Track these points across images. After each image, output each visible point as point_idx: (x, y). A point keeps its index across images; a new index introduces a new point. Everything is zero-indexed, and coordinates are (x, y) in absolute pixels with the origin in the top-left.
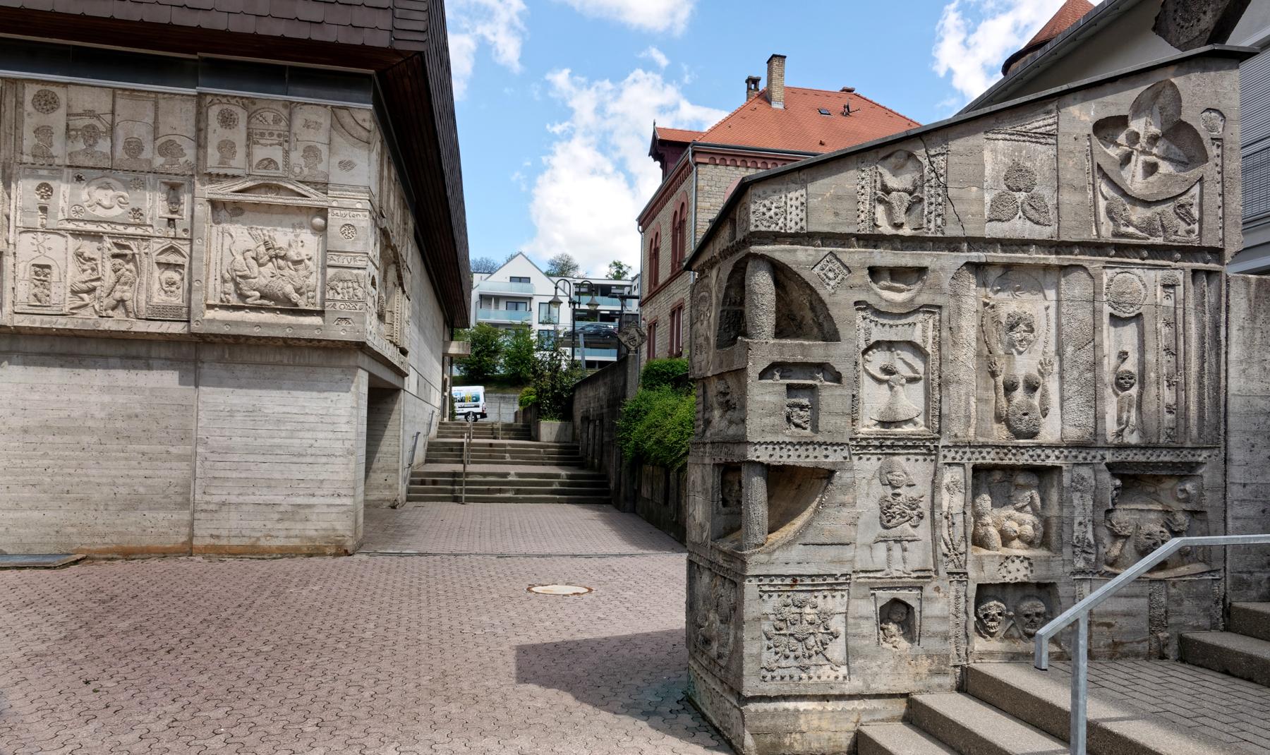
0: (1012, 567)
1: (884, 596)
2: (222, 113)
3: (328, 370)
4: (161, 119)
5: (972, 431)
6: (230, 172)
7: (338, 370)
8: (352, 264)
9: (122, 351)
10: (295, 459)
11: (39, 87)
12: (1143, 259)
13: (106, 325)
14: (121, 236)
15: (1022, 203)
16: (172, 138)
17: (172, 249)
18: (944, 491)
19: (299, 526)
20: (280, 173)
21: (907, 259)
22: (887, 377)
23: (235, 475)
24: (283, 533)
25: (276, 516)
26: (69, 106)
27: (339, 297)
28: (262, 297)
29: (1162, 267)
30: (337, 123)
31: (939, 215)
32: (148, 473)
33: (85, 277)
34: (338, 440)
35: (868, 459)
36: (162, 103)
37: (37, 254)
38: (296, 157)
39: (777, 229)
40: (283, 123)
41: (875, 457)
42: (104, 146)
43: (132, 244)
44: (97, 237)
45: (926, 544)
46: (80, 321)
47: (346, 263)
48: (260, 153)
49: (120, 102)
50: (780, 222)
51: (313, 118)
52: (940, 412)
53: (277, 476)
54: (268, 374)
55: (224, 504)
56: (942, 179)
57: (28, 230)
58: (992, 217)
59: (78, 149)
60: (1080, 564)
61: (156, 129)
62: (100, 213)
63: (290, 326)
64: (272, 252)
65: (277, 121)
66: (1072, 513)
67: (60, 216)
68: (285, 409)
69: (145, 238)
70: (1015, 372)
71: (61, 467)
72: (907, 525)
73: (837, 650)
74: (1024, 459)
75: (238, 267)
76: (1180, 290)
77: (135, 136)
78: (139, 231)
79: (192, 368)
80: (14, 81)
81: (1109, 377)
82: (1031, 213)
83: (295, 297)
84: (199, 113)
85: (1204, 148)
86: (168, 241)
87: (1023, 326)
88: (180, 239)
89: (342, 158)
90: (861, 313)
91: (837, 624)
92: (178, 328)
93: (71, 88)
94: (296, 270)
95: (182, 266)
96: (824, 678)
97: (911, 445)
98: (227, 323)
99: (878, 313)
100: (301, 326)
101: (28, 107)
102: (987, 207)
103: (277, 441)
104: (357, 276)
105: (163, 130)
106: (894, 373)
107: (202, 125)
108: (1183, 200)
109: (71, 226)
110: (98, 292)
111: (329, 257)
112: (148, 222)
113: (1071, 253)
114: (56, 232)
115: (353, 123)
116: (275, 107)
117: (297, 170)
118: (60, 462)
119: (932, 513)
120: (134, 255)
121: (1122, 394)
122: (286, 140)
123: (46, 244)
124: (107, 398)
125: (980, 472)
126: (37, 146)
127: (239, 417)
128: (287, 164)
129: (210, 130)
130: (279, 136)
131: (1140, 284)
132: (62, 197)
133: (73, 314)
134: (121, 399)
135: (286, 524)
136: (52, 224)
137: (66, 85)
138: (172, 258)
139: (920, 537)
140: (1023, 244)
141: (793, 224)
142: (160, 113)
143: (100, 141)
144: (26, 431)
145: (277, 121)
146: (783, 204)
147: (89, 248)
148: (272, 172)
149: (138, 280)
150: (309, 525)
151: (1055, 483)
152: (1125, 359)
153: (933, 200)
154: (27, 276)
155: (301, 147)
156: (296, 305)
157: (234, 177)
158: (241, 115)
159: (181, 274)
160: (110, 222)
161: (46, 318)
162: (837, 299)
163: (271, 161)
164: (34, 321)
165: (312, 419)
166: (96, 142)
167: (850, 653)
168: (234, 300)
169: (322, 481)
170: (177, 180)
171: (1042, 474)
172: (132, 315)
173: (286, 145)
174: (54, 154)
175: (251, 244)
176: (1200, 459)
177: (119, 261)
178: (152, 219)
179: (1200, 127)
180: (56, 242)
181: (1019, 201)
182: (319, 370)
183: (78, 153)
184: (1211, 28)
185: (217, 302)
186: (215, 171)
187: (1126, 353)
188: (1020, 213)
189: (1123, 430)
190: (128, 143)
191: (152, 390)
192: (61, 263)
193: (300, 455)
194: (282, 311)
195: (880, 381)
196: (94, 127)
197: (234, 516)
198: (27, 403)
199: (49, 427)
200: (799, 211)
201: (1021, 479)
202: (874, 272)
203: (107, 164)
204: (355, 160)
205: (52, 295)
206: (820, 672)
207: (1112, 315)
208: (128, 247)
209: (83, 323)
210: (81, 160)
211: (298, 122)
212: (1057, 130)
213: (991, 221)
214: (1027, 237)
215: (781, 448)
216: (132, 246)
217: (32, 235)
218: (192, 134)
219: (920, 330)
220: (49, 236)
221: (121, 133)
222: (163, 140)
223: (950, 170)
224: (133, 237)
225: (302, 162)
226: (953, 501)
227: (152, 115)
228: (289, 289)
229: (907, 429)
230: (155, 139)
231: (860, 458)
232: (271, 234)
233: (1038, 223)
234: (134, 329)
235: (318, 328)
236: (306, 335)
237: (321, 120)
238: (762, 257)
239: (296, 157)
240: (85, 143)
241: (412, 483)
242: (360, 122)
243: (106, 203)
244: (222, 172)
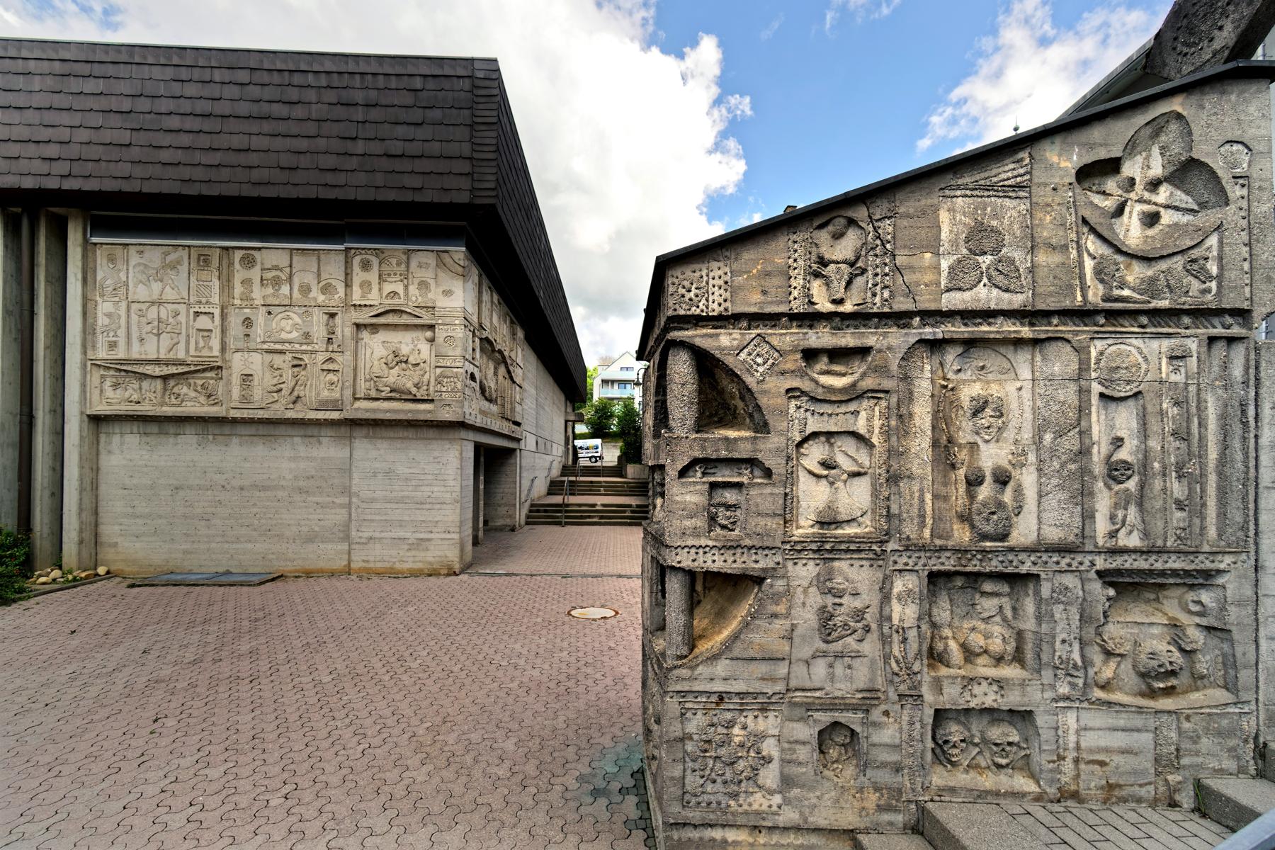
0: (977, 690)
1: (823, 719)
2: (362, 261)
3: (439, 442)
5: (927, 533)
6: (368, 303)
7: (447, 442)
8: (453, 365)
9: (302, 432)
10: (418, 506)
11: (244, 252)
12: (1143, 327)
13: (291, 415)
14: (297, 351)
15: (988, 268)
17: (330, 360)
18: (894, 601)
19: (423, 554)
20: (402, 301)
21: (848, 339)
22: (825, 472)
23: (377, 518)
24: (411, 559)
25: (406, 547)
26: (262, 264)
27: (444, 389)
28: (391, 391)
29: (1168, 335)
30: (441, 264)
31: (886, 287)
32: (321, 517)
33: (275, 381)
35: (805, 565)
36: (323, 257)
38: (413, 289)
39: (698, 312)
40: (403, 266)
41: (811, 563)
42: (285, 289)
43: (305, 357)
44: (282, 352)
45: (873, 662)
47: (449, 364)
48: (388, 288)
49: (295, 258)
50: (701, 304)
51: (424, 260)
52: (888, 512)
53: (406, 518)
54: (399, 446)
55: (371, 538)
56: (888, 246)
57: (238, 351)
58: (949, 285)
60: (1064, 689)
61: (319, 275)
62: (284, 336)
63: (410, 411)
64: (397, 359)
65: (398, 264)
66: (1054, 629)
67: (258, 340)
68: (411, 471)
69: (312, 352)
70: (980, 463)
71: (265, 514)
72: (849, 640)
73: (770, 776)
74: (994, 565)
75: (375, 369)
76: (1193, 362)
78: (310, 348)
79: (348, 443)
80: (226, 249)
81: (1098, 467)
82: (1000, 280)
83: (414, 390)
84: (346, 262)
85: (1223, 190)
86: (328, 354)
87: (988, 411)
89: (445, 288)
90: (793, 403)
91: (769, 747)
92: (335, 415)
93: (263, 251)
95: (337, 371)
96: (755, 807)
97: (854, 548)
98: (367, 410)
99: (814, 399)
100: (418, 411)
101: (237, 266)
102: (944, 274)
103: (406, 493)
104: (456, 373)
105: (323, 276)
106: (834, 468)
107: (349, 271)
108: (1195, 253)
109: (265, 346)
110: (283, 392)
113: (1050, 324)
114: (255, 350)
115: (452, 262)
116: (397, 253)
117: (414, 299)
118: (264, 510)
119: (880, 626)
121: (1117, 487)
122: (405, 277)
123: (250, 359)
124: (293, 465)
125: (935, 579)
126: (243, 293)
127: (380, 476)
128: (407, 294)
129: (354, 274)
130: (401, 275)
131: (1139, 357)
134: (302, 465)
135: (413, 553)
136: (252, 345)
137: (259, 249)
138: (331, 367)
139: (866, 653)
140: (988, 315)
141: (715, 306)
143: (283, 287)
144: (242, 489)
145: (398, 264)
146: (704, 283)
148: (396, 301)
150: (429, 554)
151: (1031, 592)
152: (1119, 447)
153: (879, 270)
154: (238, 383)
155: (416, 281)
157: (371, 306)
158: (375, 261)
160: (290, 343)
161: (251, 411)
162: (765, 386)
163: (396, 293)
165: (430, 477)
166: (280, 288)
167: (787, 782)
168: (373, 394)
169: (437, 522)
171: (1017, 580)
173: (405, 281)
175: (384, 353)
176: (1222, 566)
177: (296, 369)
179: (1218, 165)
180: (256, 358)
181: (984, 267)
182: (434, 442)
183: (268, 296)
184: (1231, 44)
185: (362, 396)
186: (358, 303)
187: (1122, 440)
188: (985, 280)
189: (1117, 531)
190: (301, 286)
191: (323, 459)
192: (260, 373)
193: (422, 503)
194: (406, 400)
195: (818, 477)
196: (278, 277)
197: (378, 546)
199: (257, 486)
200: (722, 291)
201: (988, 587)
202: (810, 355)
203: (287, 302)
204: (453, 289)
206: (752, 799)
207: (1102, 395)
210: (270, 301)
211: (413, 264)
212: (1030, 180)
213: (949, 290)
214: (993, 307)
215: (705, 553)
217: (240, 354)
218: (343, 278)
219: (867, 418)
221: (297, 281)
222: (324, 283)
223: (899, 235)
224: (305, 352)
225: (417, 292)
226: (904, 613)
228: (409, 385)
229: (850, 530)
231: (795, 564)
233: (1007, 290)
234: (308, 417)
235: (430, 412)
236: (422, 417)
237: (430, 261)
238: (683, 345)
239: (413, 289)
240: (273, 287)
241: (531, 511)
244: (362, 303)
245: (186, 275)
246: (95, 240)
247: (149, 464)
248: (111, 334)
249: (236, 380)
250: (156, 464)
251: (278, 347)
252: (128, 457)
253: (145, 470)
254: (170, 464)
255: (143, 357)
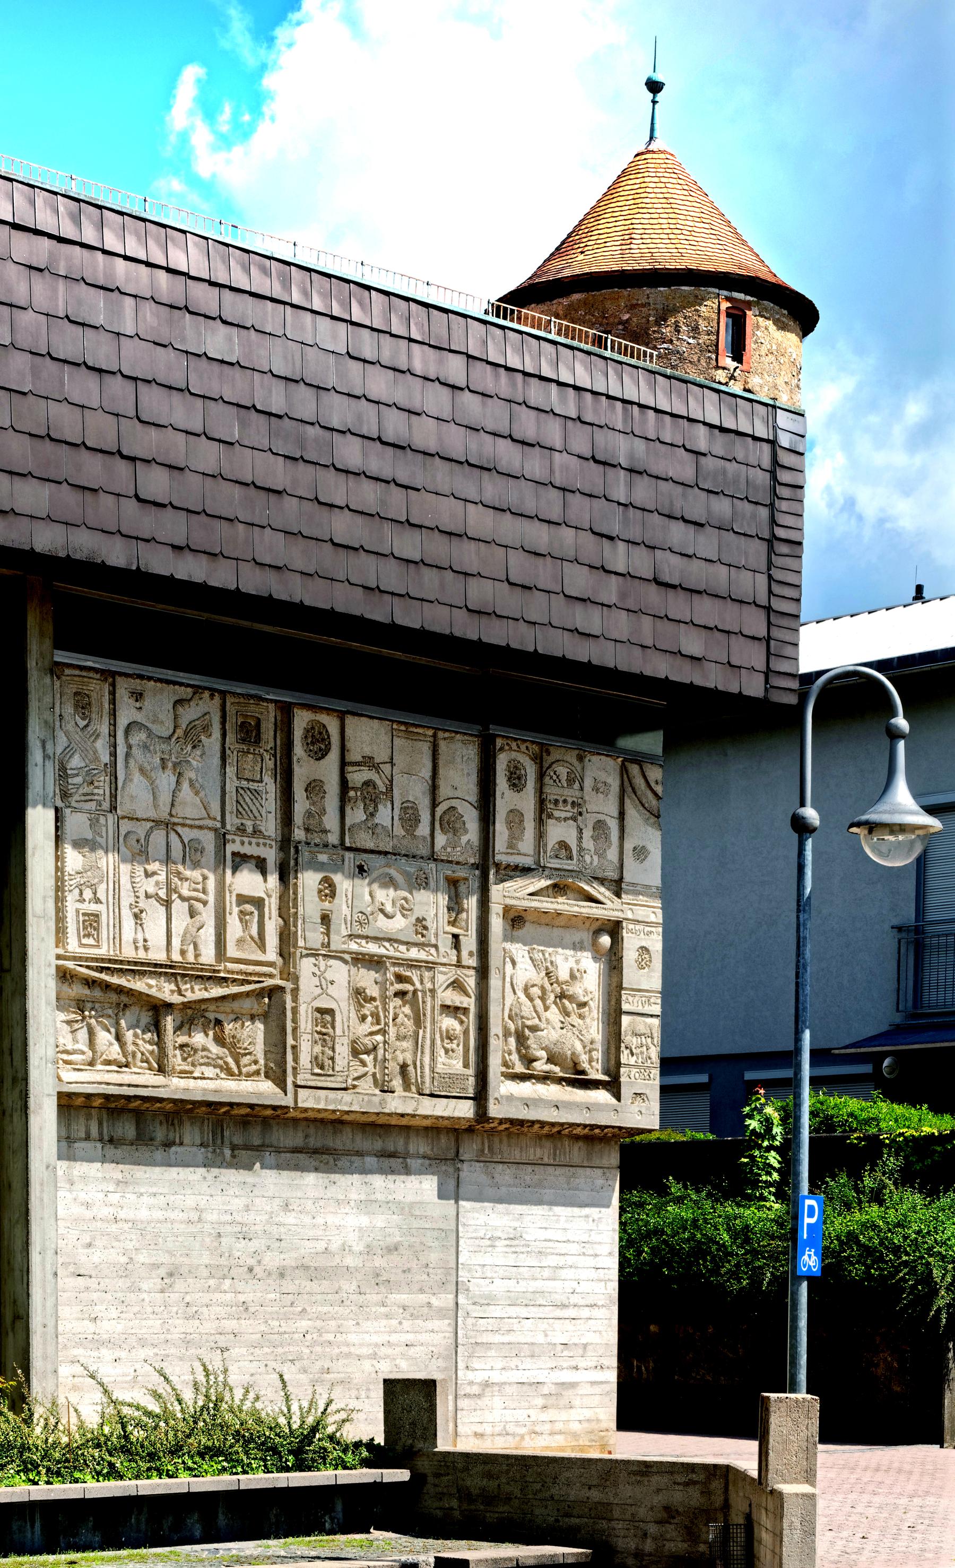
4: (442, 771)
7: (599, 1172)
16: (454, 803)
23: (497, 1338)
25: (540, 1402)
32: (410, 1337)
34: (601, 1281)
37: (319, 991)
43: (414, 975)
44: (374, 963)
46: (366, 1098)
53: (540, 1339)
55: (486, 1385)
59: (358, 821)
61: (434, 788)
62: (382, 923)
68: (550, 1234)
69: (430, 966)
77: (411, 799)
78: (422, 955)
88: (463, 967)
94: (581, 1017)
109: (353, 946)
111: (624, 997)
112: (433, 941)
120: (415, 992)
132: (344, 899)
133: (354, 1087)
135: (551, 1414)
142: (441, 763)
143: (380, 807)
147: (367, 979)
149: (421, 1032)
156: (583, 1072)
159: (462, 1022)
164: (318, 1100)
166: (376, 809)
169: (585, 1346)
170: (461, 873)
172: (413, 1088)
174: (328, 828)
178: (436, 935)
182: (580, 1171)
198: (282, 1229)
199: (306, 1268)
205: (337, 1056)
208: (407, 980)
209: (369, 1101)
216: (416, 980)
217: (312, 960)
220: (332, 962)
224: (413, 964)
227: (429, 765)
230: (434, 805)
232: (553, 959)
237: (610, 780)
242: (653, 785)
243: (389, 908)
245: (216, 761)
246: (61, 656)
247: (122, 1215)
248: (88, 894)
249: (306, 1022)
250: (131, 1216)
251: (373, 948)
252: (82, 1196)
253: (114, 1228)
254: (158, 1215)
255: (142, 955)
